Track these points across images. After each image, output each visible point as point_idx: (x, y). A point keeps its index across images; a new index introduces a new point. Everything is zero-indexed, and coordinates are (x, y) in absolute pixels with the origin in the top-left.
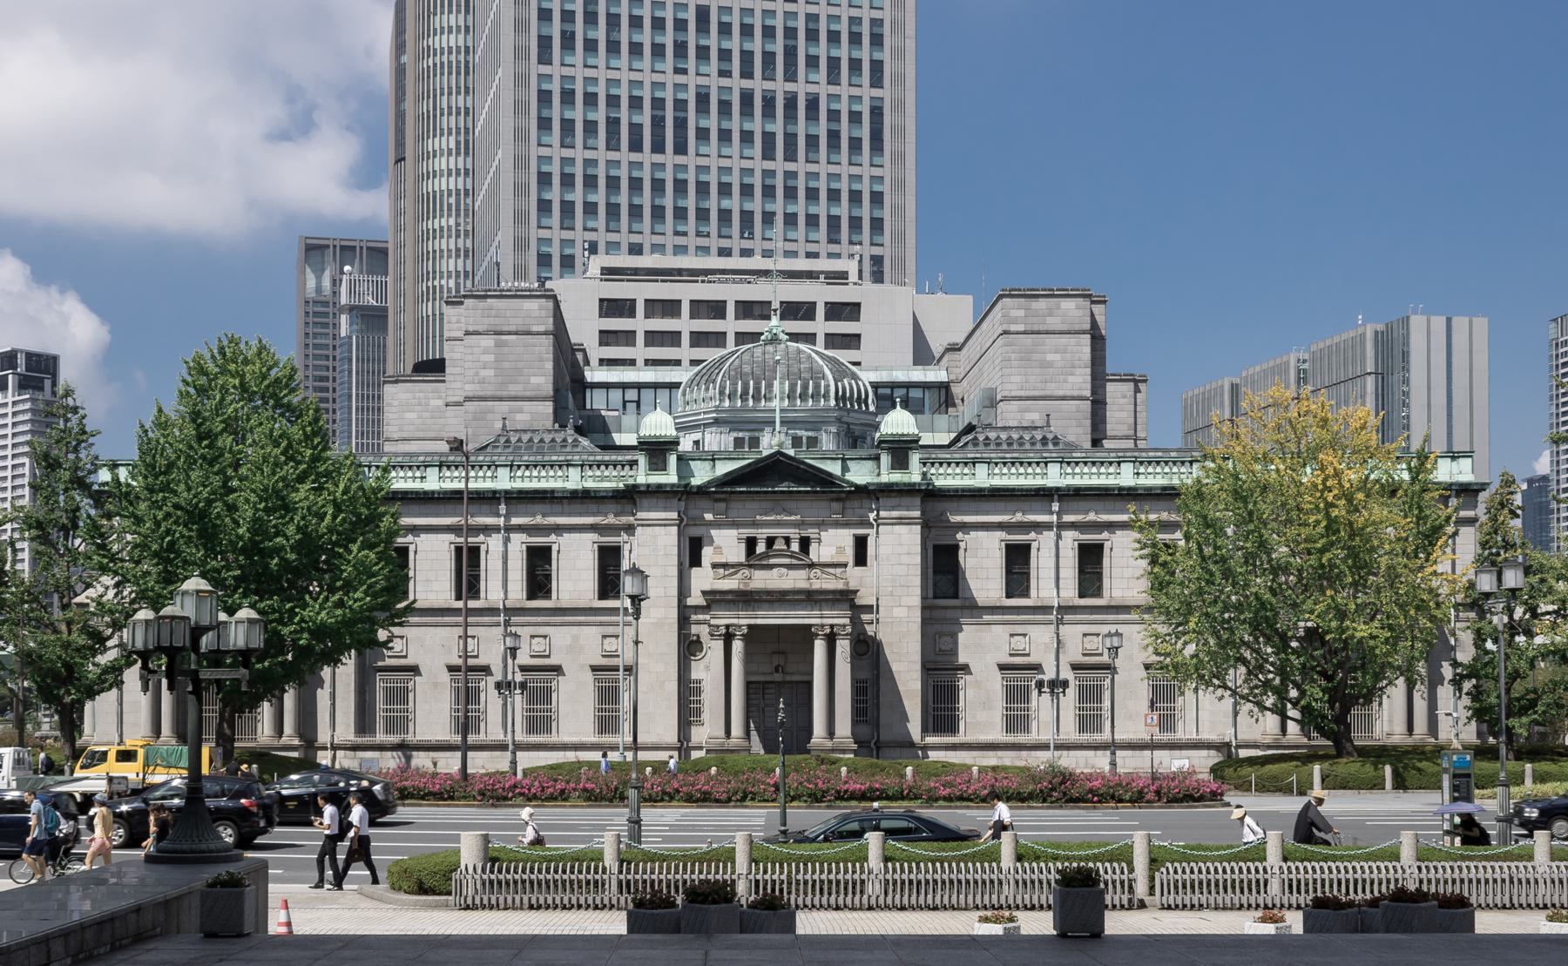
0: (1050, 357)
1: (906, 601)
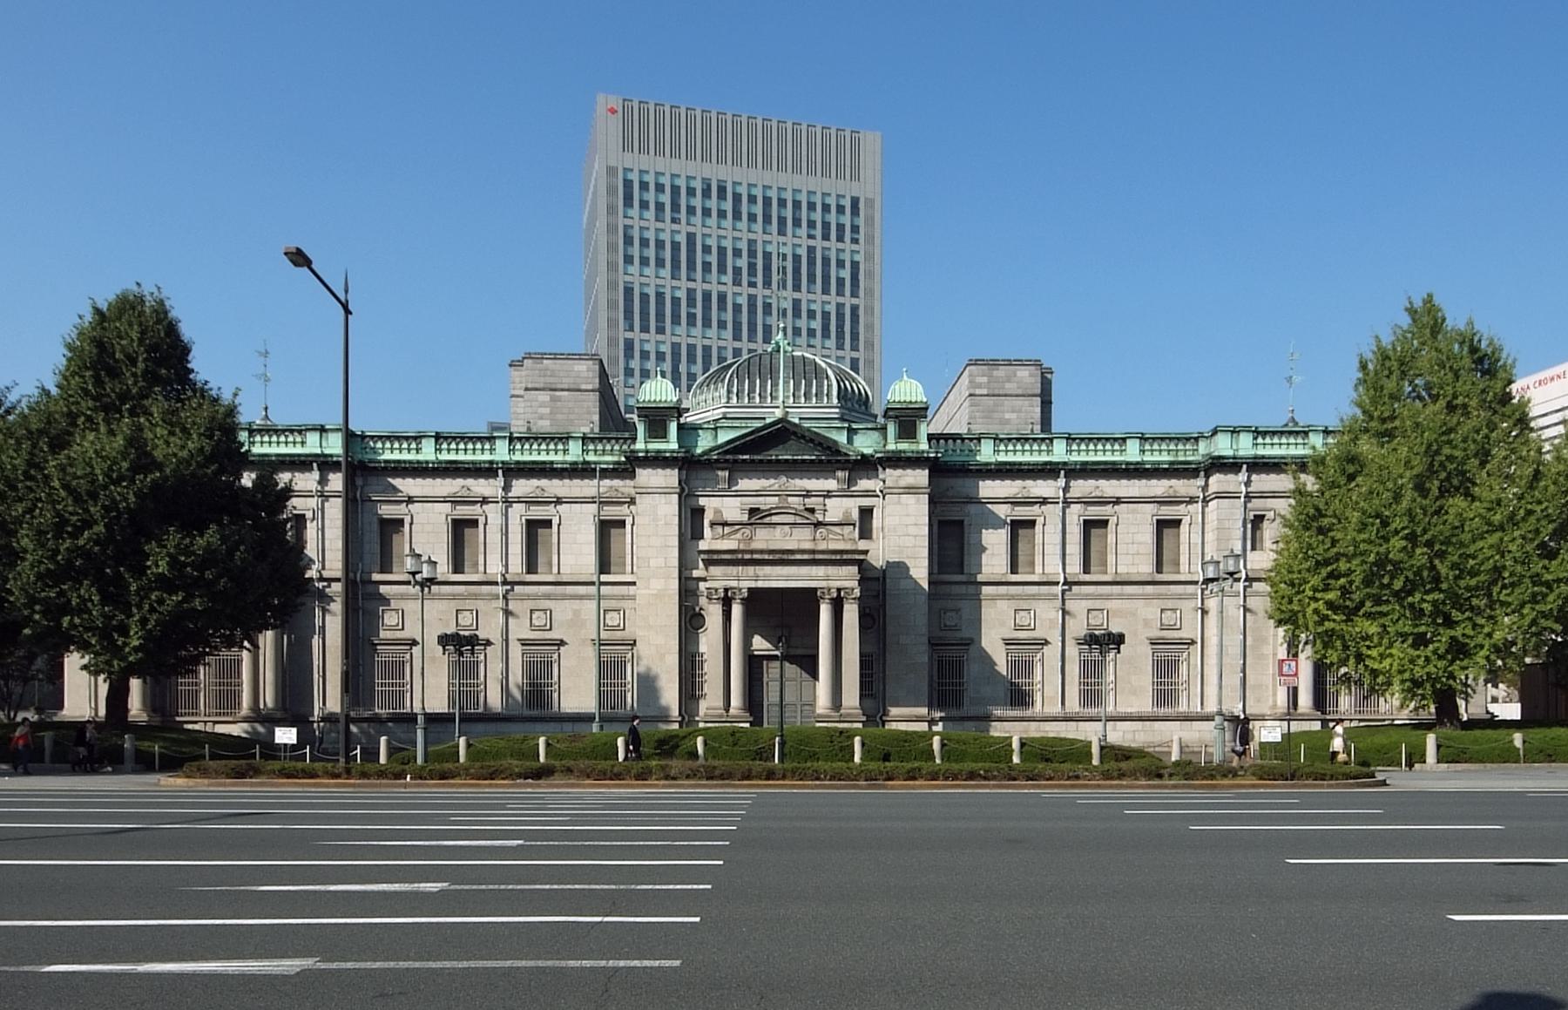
0: (1007, 416)
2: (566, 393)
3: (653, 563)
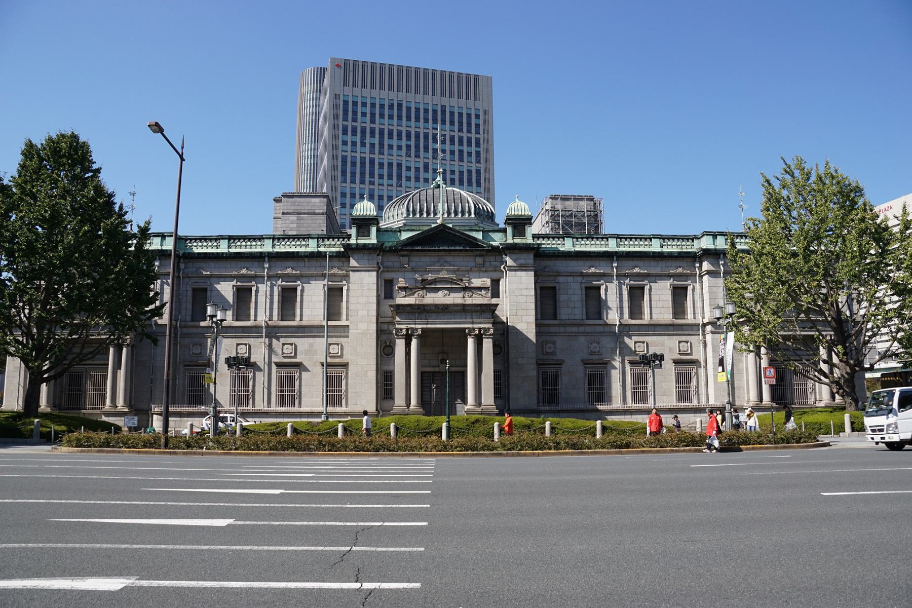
1: (525, 318)
2: (306, 216)
3: (360, 313)
